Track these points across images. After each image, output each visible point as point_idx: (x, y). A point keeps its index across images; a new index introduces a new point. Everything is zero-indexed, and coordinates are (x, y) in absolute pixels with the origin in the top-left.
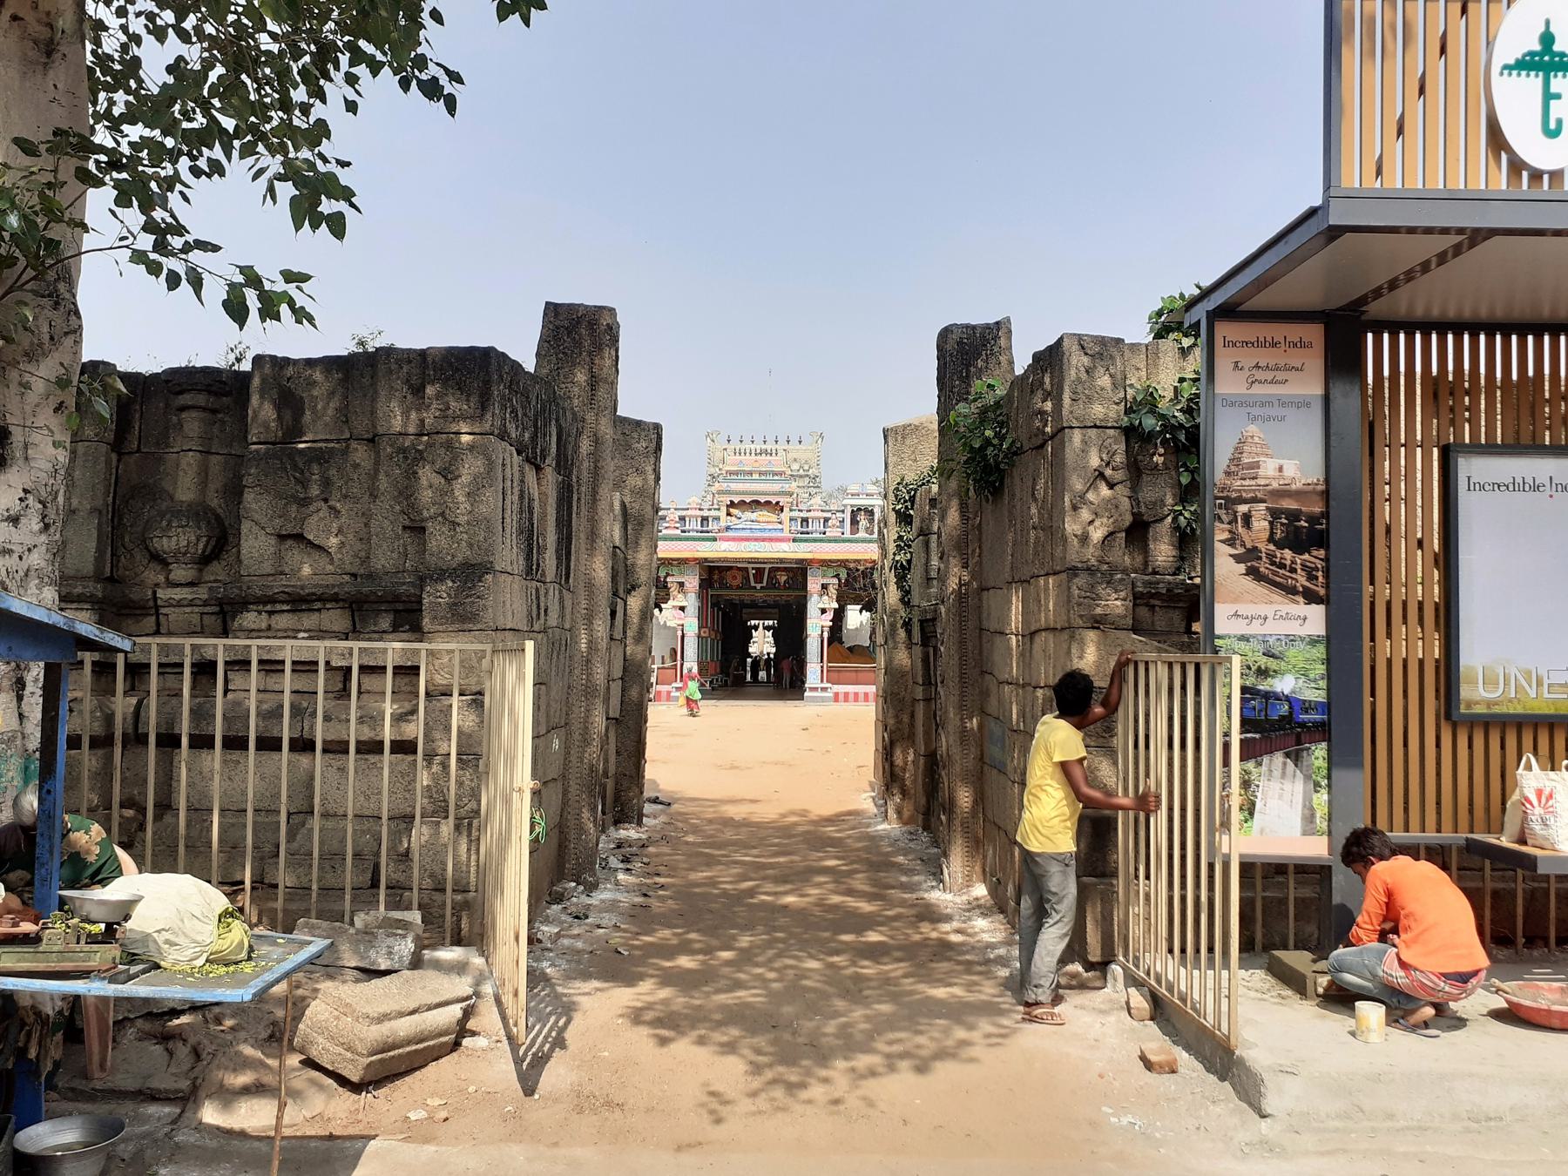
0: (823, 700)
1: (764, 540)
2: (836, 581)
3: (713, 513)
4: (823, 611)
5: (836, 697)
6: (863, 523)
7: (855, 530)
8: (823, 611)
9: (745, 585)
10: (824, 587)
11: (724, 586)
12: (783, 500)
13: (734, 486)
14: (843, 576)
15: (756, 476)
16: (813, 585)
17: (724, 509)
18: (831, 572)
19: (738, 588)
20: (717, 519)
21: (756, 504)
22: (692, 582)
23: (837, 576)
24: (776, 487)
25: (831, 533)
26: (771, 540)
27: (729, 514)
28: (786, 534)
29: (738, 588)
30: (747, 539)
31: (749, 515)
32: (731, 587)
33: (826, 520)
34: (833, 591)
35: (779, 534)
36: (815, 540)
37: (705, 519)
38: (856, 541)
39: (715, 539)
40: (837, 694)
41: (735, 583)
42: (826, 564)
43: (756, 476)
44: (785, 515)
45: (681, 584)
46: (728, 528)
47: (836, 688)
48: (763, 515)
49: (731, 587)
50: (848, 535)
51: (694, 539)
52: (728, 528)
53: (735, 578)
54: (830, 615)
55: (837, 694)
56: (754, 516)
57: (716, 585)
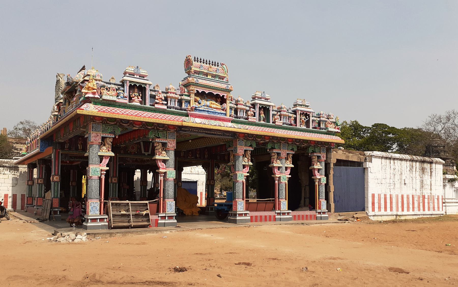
0: (246, 221)
1: (212, 118)
5: (251, 220)
8: (244, 166)
13: (200, 81)
19: (135, 154)
20: (189, 102)
21: (211, 96)
25: (251, 119)
32: (131, 153)
35: (223, 116)
36: (241, 123)
39: (187, 115)
42: (247, 137)
44: (228, 105)
46: (196, 109)
49: (131, 153)
51: (173, 113)
52: (196, 109)
56: (208, 103)
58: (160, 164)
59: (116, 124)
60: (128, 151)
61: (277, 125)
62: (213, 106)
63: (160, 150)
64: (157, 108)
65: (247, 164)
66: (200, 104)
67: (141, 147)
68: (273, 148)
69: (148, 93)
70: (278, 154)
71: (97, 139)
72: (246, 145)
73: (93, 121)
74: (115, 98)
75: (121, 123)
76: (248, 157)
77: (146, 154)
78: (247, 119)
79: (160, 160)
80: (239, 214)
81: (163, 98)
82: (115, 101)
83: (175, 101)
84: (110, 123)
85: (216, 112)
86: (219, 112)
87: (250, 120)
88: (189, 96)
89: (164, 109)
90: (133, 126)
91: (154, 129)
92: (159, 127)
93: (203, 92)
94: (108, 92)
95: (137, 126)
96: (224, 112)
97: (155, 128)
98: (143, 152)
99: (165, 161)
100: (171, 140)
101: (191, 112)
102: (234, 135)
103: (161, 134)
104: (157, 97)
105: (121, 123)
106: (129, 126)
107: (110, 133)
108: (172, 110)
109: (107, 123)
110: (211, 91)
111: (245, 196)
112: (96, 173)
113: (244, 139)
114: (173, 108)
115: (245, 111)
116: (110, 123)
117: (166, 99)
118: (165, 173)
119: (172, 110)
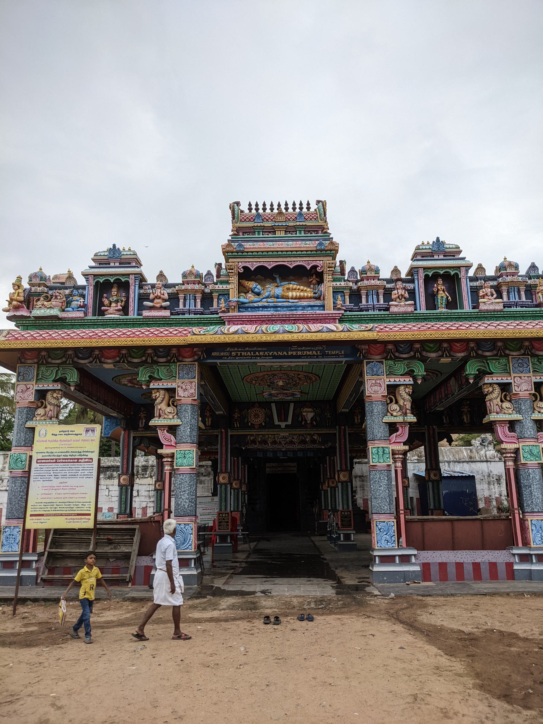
2: (409, 380)
3: (220, 287)
4: (393, 428)
5: (426, 571)
6: (443, 295)
7: (431, 303)
9: (269, 424)
10: (392, 389)
11: (245, 426)
12: (321, 262)
14: (420, 370)
15: (280, 234)
16: (375, 387)
17: (234, 280)
18: (401, 368)
19: (261, 427)
21: (283, 273)
22: (188, 389)
23: (410, 373)
24: (312, 245)
25: (399, 307)
26: (306, 320)
27: (242, 289)
28: (330, 311)
29: (261, 427)
30: (270, 320)
31: (272, 289)
32: (253, 427)
33: (388, 294)
34: (405, 397)
36: (373, 320)
37: (207, 299)
38: (438, 318)
39: (222, 322)
40: (426, 566)
41: (257, 421)
43: (280, 234)
44: (327, 287)
45: (171, 392)
46: (241, 306)
47: (435, 557)
48: (295, 290)
49: (253, 427)
50: (422, 310)
52: (241, 306)
53: (256, 416)
54: (404, 434)
55: (426, 566)
56: (279, 291)
58: (163, 435)
59: (64, 363)
60: (248, 422)
61: (487, 311)
62: (290, 294)
63: (163, 406)
64: (147, 318)
65: (400, 419)
66: (258, 294)
67: (272, 412)
68: (482, 374)
69: (134, 292)
70: (505, 388)
71: (26, 395)
72: (390, 374)
73: (21, 363)
74: (55, 312)
75: (76, 359)
76: (401, 402)
77: (283, 424)
78: (387, 309)
79: (162, 427)
80: (380, 557)
81: (166, 296)
82: (56, 317)
83: (195, 299)
84: (53, 361)
85: (295, 306)
86: (305, 303)
87: (393, 309)
88: (227, 282)
89: (164, 317)
90: (101, 362)
91: (145, 362)
92: (159, 357)
93: (261, 269)
94: (46, 303)
95: (109, 361)
96: (318, 303)
97: (149, 360)
98: (277, 422)
99: (172, 429)
100: (186, 381)
101: (230, 314)
102: (357, 353)
103: (162, 371)
104: (152, 296)
105: (76, 359)
106: (91, 362)
107: (55, 381)
108: (187, 316)
109: (47, 363)
110: (281, 261)
111: (402, 507)
112: (19, 465)
113: (386, 359)
114: (189, 312)
115: (381, 291)
116: (53, 361)
117: (174, 298)
118: (172, 456)
119: (187, 316)
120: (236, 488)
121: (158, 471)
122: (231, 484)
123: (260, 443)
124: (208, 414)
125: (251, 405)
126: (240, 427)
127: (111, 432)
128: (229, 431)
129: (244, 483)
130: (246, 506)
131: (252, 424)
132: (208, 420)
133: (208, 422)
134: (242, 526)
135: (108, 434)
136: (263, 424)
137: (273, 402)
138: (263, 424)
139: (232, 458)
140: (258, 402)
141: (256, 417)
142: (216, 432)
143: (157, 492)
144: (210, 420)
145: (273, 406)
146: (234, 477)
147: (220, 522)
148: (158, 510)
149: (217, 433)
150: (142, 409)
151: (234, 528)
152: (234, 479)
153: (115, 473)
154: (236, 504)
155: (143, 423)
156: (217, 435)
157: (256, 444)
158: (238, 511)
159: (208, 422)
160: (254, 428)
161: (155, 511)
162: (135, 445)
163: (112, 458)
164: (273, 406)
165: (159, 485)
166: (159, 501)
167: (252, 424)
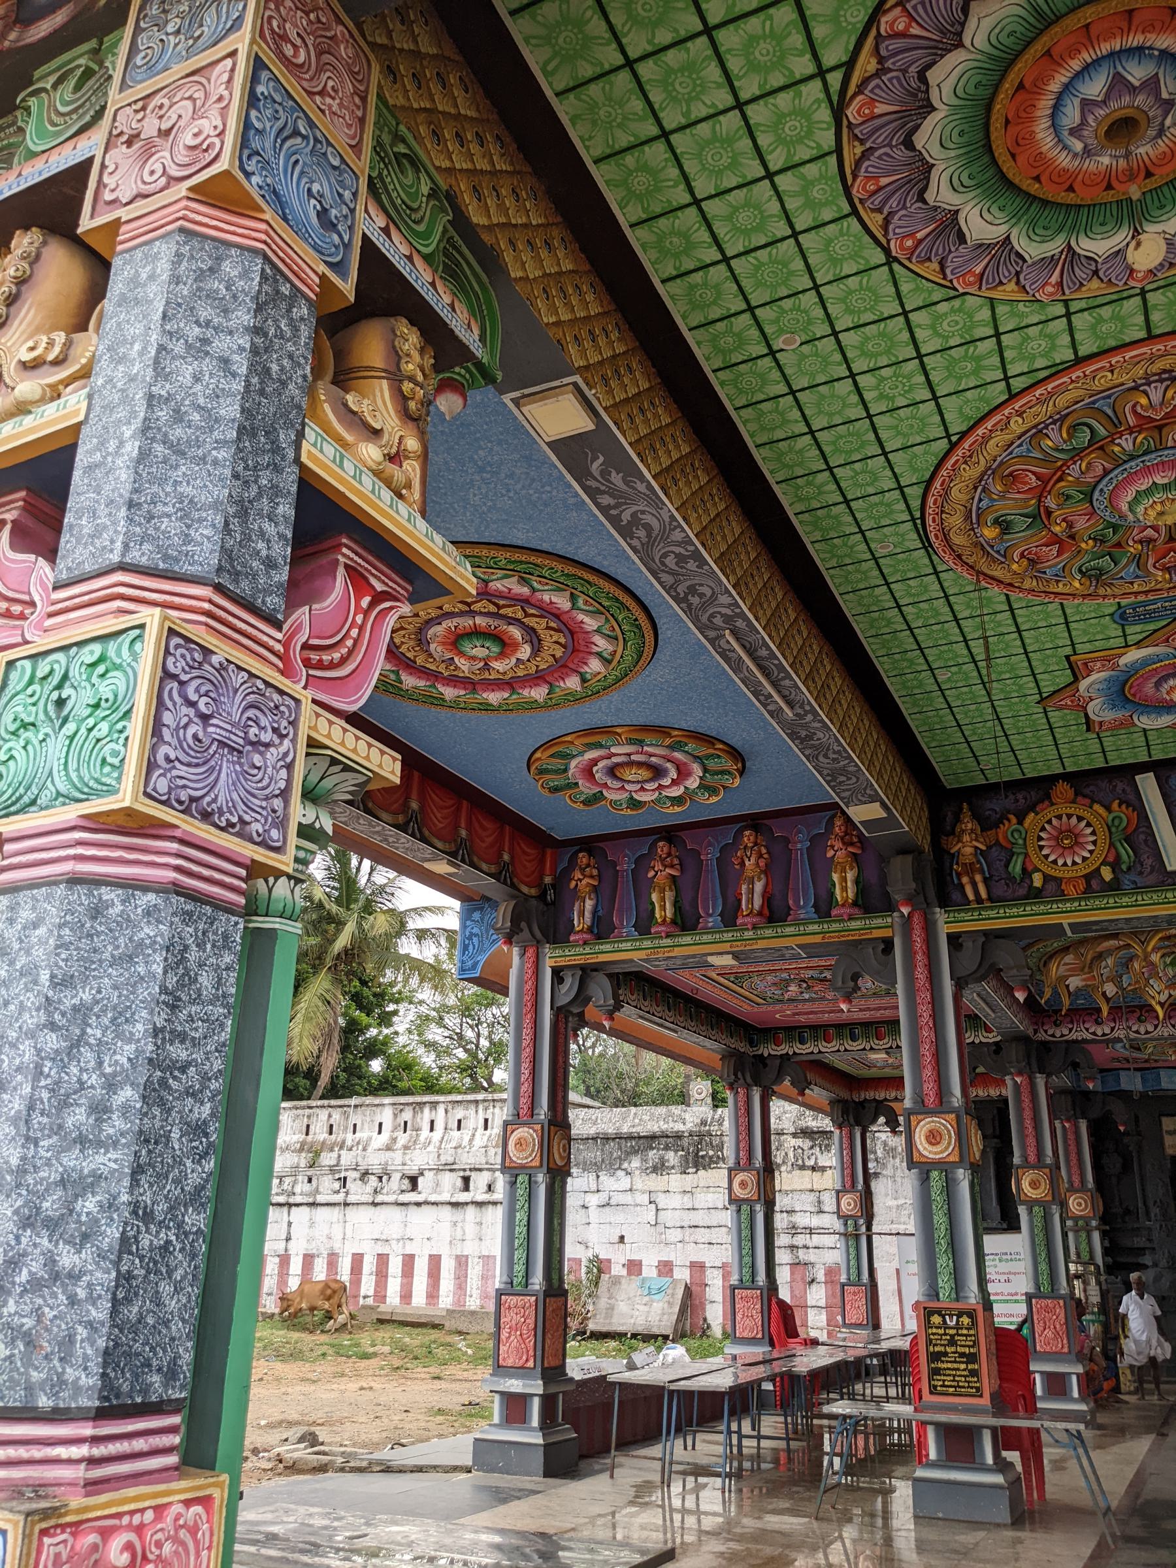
19: (1091, 885)
49: (1054, 889)
53: (1068, 839)
57: (973, 887)
60: (1026, 873)
67: (1143, 817)
120: (1037, 1202)
121: (738, 1133)
122: (1063, 1205)
123: (1117, 1012)
124: (837, 851)
125: (1036, 790)
126: (990, 899)
127: (482, 959)
128: (940, 916)
129: (1083, 1188)
130: (1098, 1273)
131: (1047, 878)
132: (844, 879)
133: (844, 889)
134: (1080, 1357)
135: (474, 967)
136: (1107, 874)
137: (1143, 768)
138: (1107, 874)
139: (1057, 1123)
140: (1067, 777)
141: (1065, 844)
142: (879, 926)
143: (739, 1211)
144: (850, 876)
145: (1148, 784)
146: (1071, 1182)
147: (935, 1357)
148: (747, 1277)
149: (887, 933)
150: (583, 858)
151: (1013, 1390)
152: (1072, 1189)
153: (672, 1154)
154: (1043, 1267)
155: (588, 915)
156: (888, 944)
157: (1098, 1023)
158: (1053, 1294)
159: (844, 889)
160: (1061, 895)
161: (734, 1279)
162: (563, 1001)
163: (662, 1110)
164: (1148, 784)
165: (743, 1184)
166: (747, 1245)
167: (1047, 878)
